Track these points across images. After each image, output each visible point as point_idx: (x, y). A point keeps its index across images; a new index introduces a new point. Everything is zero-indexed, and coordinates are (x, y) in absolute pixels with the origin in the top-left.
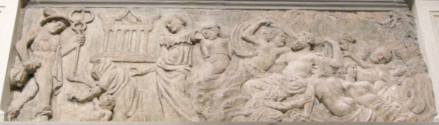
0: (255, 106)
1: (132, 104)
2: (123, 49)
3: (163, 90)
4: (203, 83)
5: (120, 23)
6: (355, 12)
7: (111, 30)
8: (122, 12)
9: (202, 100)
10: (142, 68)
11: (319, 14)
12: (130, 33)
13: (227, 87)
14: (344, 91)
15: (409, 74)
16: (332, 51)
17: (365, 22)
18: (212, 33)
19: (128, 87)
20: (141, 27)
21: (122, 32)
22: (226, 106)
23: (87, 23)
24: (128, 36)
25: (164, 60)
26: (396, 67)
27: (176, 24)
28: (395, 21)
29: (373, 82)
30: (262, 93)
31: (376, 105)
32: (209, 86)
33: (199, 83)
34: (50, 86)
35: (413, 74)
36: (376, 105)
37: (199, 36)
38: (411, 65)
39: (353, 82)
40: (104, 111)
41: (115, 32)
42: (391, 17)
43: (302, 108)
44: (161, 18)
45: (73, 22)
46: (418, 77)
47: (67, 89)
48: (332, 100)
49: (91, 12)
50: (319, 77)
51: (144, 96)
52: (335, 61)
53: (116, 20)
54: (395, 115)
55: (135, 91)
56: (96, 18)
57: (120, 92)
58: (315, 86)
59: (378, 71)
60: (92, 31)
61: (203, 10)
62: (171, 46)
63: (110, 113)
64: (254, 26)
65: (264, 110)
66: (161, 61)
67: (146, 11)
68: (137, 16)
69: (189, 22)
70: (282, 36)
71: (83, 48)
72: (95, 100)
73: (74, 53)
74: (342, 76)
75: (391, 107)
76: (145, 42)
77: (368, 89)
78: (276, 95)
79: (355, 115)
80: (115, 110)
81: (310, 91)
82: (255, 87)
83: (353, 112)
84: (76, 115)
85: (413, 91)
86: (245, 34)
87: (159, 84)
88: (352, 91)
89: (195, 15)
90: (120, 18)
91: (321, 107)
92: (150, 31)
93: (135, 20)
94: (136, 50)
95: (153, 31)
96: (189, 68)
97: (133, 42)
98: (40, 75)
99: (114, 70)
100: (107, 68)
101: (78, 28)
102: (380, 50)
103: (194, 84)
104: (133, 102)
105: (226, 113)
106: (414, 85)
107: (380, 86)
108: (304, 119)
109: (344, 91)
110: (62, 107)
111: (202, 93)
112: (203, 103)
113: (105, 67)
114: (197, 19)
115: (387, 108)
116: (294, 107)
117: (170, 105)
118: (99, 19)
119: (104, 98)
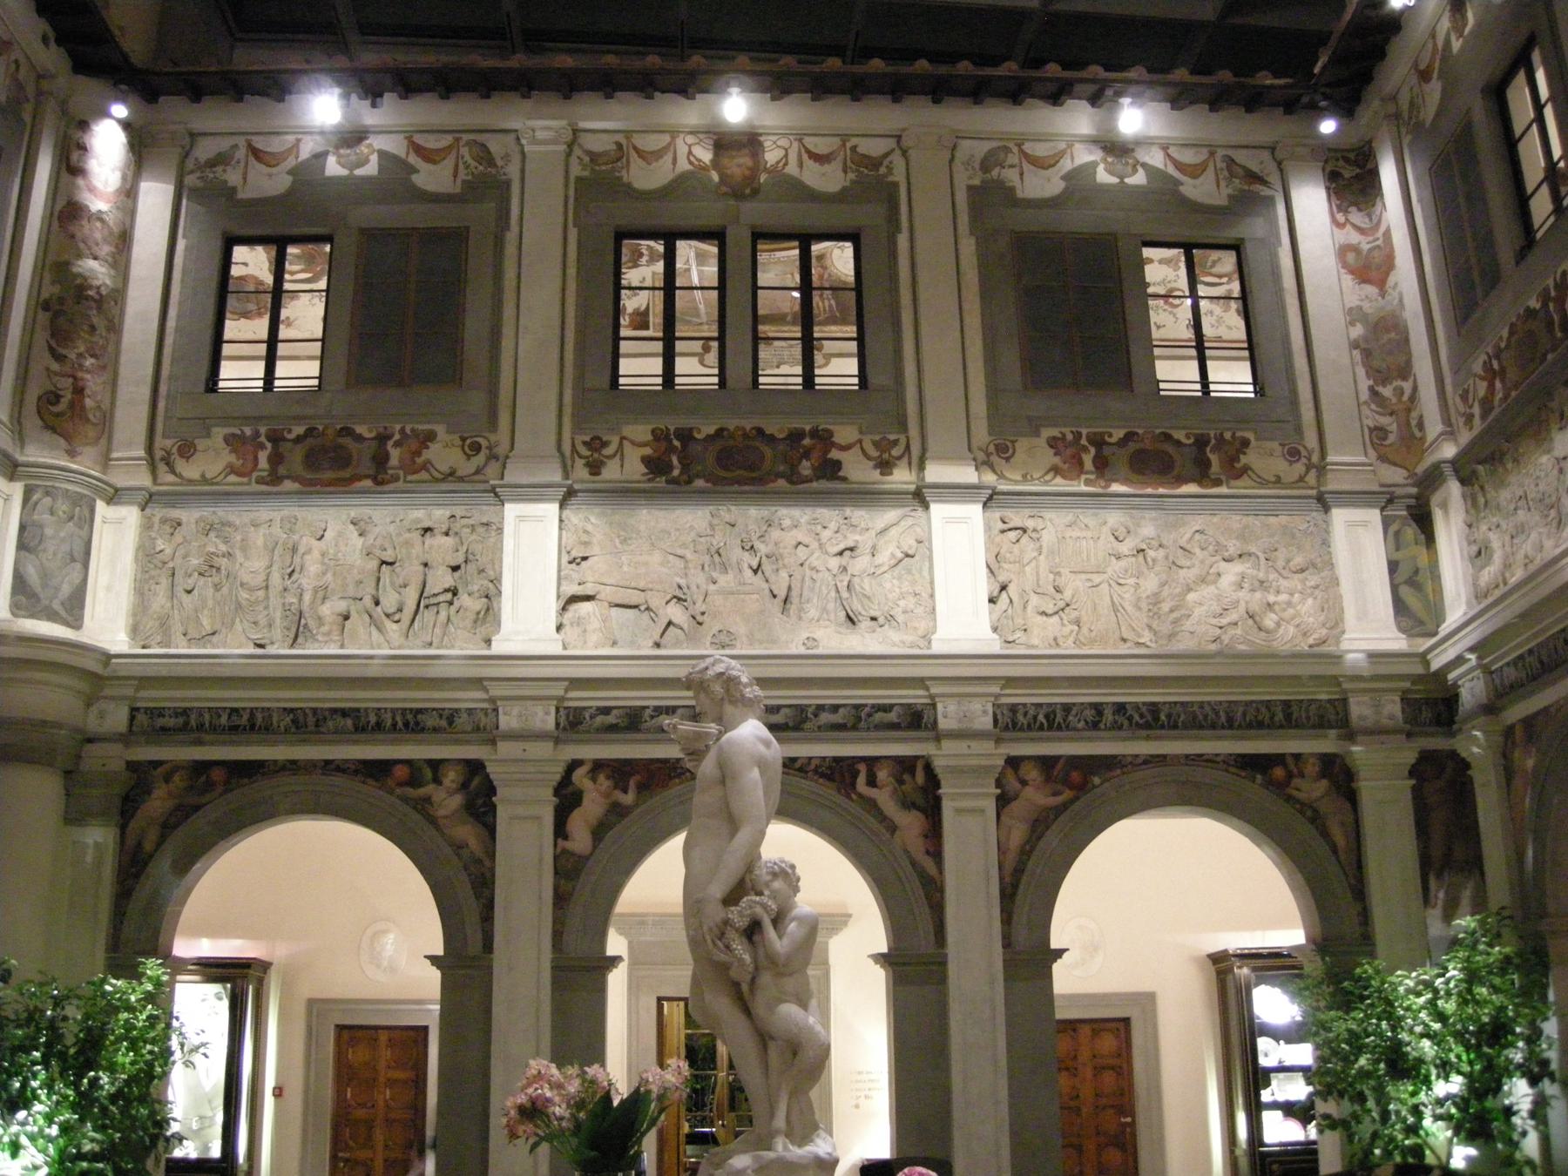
0: (1199, 623)
11: (1245, 519)
17: (1285, 527)
18: (1155, 543)
20: (1089, 534)
26: (1313, 580)
27: (1121, 533)
29: (1292, 595)
32: (1156, 600)
47: (1034, 600)
52: (1261, 575)
59: (1295, 582)
60: (1048, 537)
64: (1188, 536)
69: (1132, 528)
73: (1033, 564)
74: (1266, 590)
77: (1289, 604)
81: (1242, 608)
86: (1183, 542)
88: (1276, 607)
91: (1250, 622)
98: (1012, 589)
102: (1299, 560)
114: (1139, 525)
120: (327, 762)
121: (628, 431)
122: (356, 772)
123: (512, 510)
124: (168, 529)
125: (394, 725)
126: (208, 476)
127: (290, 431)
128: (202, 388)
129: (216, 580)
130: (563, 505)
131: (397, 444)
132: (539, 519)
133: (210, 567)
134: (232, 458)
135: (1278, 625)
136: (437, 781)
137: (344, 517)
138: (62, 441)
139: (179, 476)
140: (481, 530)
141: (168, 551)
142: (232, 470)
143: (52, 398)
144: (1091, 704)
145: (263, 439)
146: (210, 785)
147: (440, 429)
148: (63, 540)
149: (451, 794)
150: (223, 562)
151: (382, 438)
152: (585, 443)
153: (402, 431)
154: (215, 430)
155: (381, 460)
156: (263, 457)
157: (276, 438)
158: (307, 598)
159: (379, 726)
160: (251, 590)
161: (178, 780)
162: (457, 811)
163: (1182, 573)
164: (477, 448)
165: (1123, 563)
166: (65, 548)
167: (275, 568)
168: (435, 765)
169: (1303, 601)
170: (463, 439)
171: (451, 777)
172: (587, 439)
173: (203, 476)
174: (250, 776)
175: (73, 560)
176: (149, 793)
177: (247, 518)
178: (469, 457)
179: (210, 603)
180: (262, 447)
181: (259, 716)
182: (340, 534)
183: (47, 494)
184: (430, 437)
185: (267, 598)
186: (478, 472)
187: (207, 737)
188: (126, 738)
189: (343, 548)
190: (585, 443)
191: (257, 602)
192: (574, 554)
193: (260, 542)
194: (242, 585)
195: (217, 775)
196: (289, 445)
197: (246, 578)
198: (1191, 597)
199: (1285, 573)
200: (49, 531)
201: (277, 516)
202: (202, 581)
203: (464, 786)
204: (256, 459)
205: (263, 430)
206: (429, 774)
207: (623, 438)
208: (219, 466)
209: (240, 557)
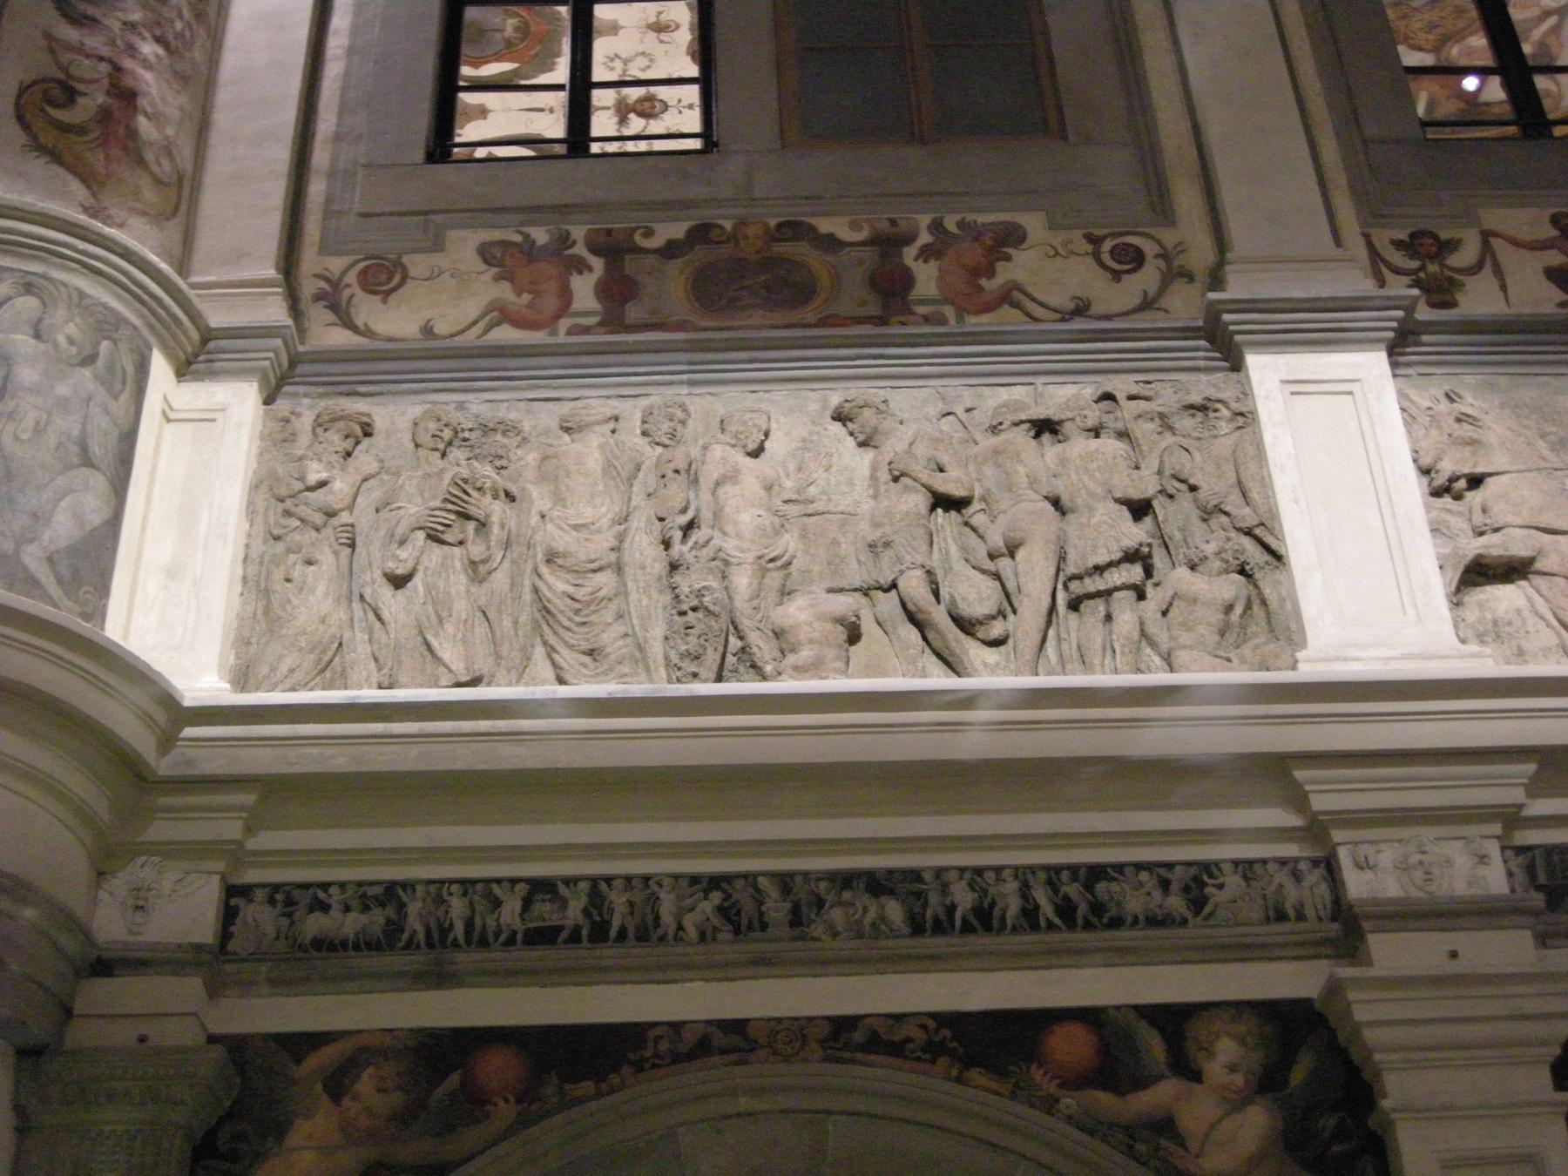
120: (842, 1025)
121: (1496, 218)
122: (933, 1050)
123: (1266, 371)
124: (335, 440)
125: (1030, 914)
126: (441, 328)
127: (649, 233)
128: (419, 154)
129: (476, 550)
130: (1395, 350)
131: (926, 253)
132: (1344, 388)
133: (455, 518)
134: (505, 291)
136: (1185, 1068)
137: (813, 407)
138: (76, 186)
139: (368, 333)
140: (1186, 423)
141: (341, 487)
142: (502, 314)
143: (57, 92)
145: (580, 250)
146: (474, 1101)
147: (1034, 224)
148: (63, 404)
149: (1237, 1104)
150: (497, 510)
151: (889, 243)
152: (1398, 244)
153: (937, 227)
154: (452, 235)
155: (892, 290)
156: (584, 290)
157: (613, 249)
158: (742, 581)
159: (985, 918)
160: (579, 572)
161: (372, 1092)
162: (1255, 1161)
164: (1136, 259)
166: (67, 424)
167: (639, 521)
168: (1173, 1020)
170: (1096, 241)
171: (1227, 1055)
172: (1403, 235)
173: (427, 331)
174: (600, 1077)
175: (88, 462)
176: (279, 1130)
177: (548, 416)
178: (1117, 276)
179: (461, 607)
180: (581, 266)
181: (618, 900)
182: (806, 445)
183: (28, 288)
184: (1012, 237)
185: (622, 592)
186: (1147, 305)
187: (466, 959)
188: (217, 961)
189: (819, 475)
190: (1398, 244)
191: (596, 601)
192: (1447, 467)
193: (594, 461)
194: (551, 558)
195: (497, 1068)
196: (651, 260)
197: (563, 540)
200: (26, 374)
201: (633, 412)
202: (437, 551)
203: (1268, 1082)
204: (566, 295)
205: (579, 232)
206: (1154, 1047)
207: (1486, 235)
208: (472, 308)
209: (539, 497)
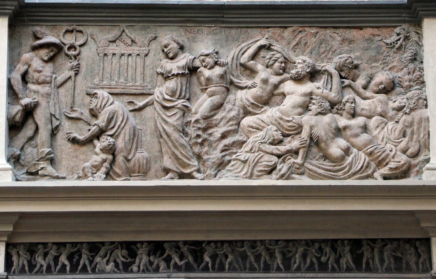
1: (132, 146)
2: (119, 78)
3: (161, 130)
4: (201, 121)
5: (115, 45)
6: (361, 28)
7: (105, 54)
8: (115, 32)
9: (200, 140)
10: (140, 102)
11: (322, 32)
12: (126, 58)
13: (225, 125)
14: (339, 132)
15: (408, 111)
16: (331, 81)
19: (127, 127)
21: (117, 57)
22: (224, 148)
23: (81, 46)
24: (124, 58)
25: (161, 94)
28: (401, 40)
30: (258, 135)
31: (369, 150)
33: (197, 121)
34: (50, 126)
35: (412, 110)
36: (369, 150)
37: (197, 63)
38: (411, 98)
39: (349, 119)
40: (104, 156)
41: (110, 57)
42: (398, 35)
43: (296, 153)
44: (157, 39)
45: (65, 45)
46: (417, 114)
48: (327, 145)
49: (84, 31)
50: (316, 115)
51: (143, 134)
52: (333, 95)
53: (110, 42)
54: (387, 160)
55: (134, 130)
56: (89, 39)
57: (120, 133)
58: (311, 128)
61: (200, 28)
62: (169, 77)
63: (110, 157)
65: (260, 156)
66: (159, 95)
67: (141, 30)
68: (132, 37)
69: (187, 44)
70: (282, 63)
71: (79, 78)
72: (96, 142)
73: (70, 84)
75: (384, 152)
76: (142, 70)
77: (365, 128)
78: (272, 138)
79: (348, 162)
80: (116, 153)
82: (252, 127)
83: (347, 157)
84: (77, 157)
85: (409, 131)
86: (244, 59)
87: (158, 123)
89: (192, 35)
90: (114, 39)
92: (146, 55)
93: (129, 42)
94: (132, 79)
95: (149, 55)
96: (187, 104)
97: (130, 69)
99: (112, 106)
100: (105, 105)
101: (72, 53)
102: (382, 77)
103: (192, 122)
104: (132, 143)
105: (223, 156)
106: (411, 124)
107: (376, 125)
108: (298, 166)
109: (339, 132)
110: (63, 147)
111: (200, 133)
112: (202, 144)
113: (103, 104)
114: (194, 40)
115: (379, 154)
116: (288, 152)
117: (169, 147)
118: (93, 41)
119: (105, 141)
135: (347, 152)
144: (121, 243)
163: (241, 94)
165: (171, 84)
169: (381, 126)
198: (247, 121)
199: (368, 94)
